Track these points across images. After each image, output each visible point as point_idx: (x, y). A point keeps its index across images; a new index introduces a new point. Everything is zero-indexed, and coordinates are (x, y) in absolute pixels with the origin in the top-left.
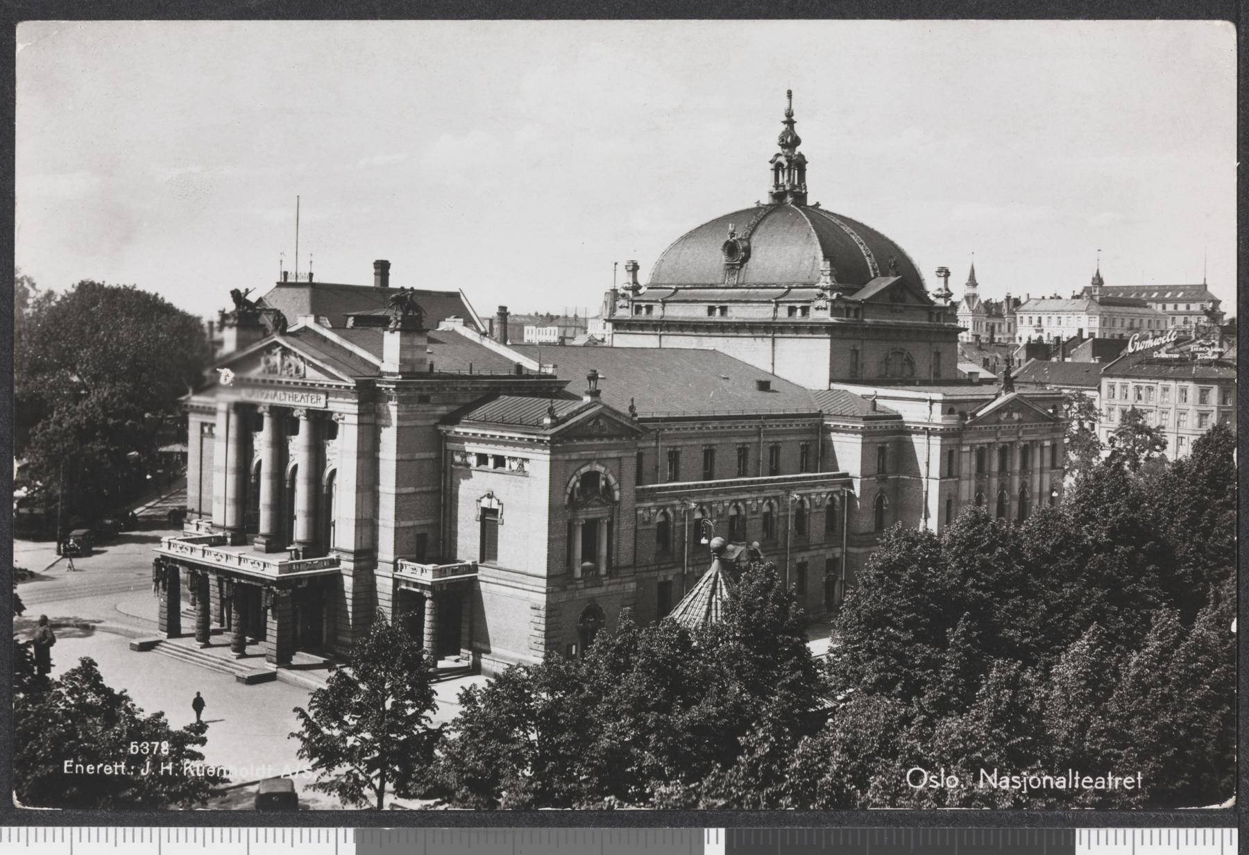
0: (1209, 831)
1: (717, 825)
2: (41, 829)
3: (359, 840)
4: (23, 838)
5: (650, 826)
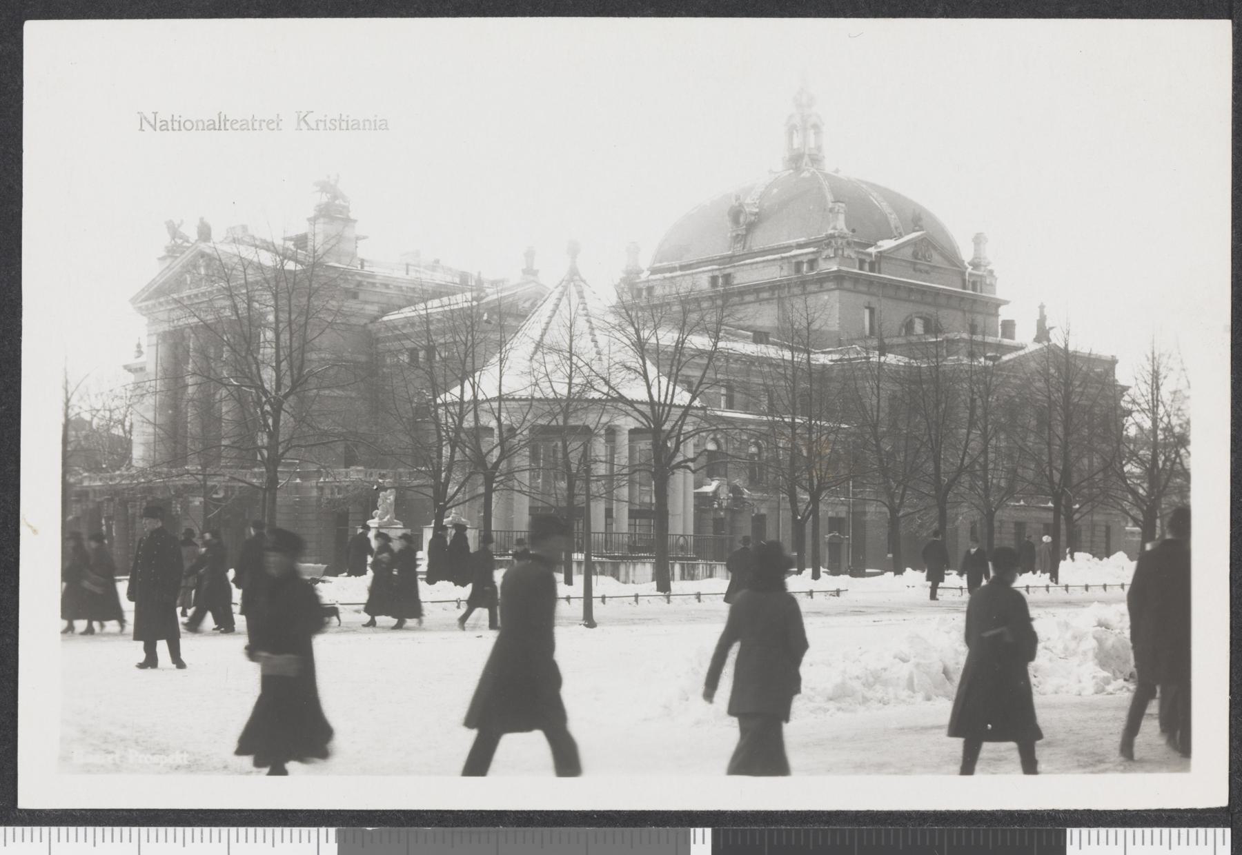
0: (1201, 830)
2: (19, 829)
3: (340, 840)
5: (636, 826)
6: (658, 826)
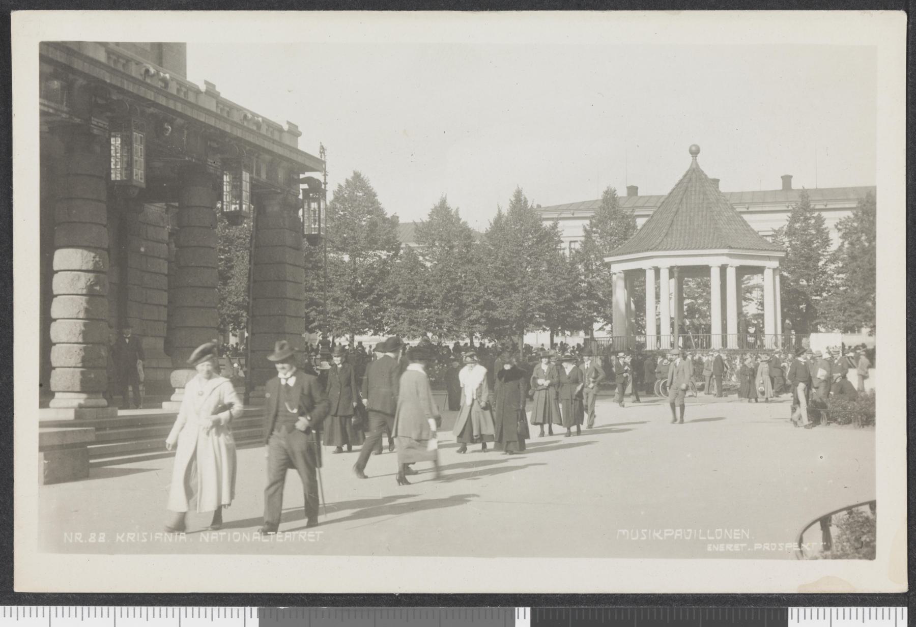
0: (886, 609)
1: (524, 605)
2: (27, 608)
3: (261, 616)
4: (14, 614)
5: (475, 605)
6: (491, 605)
